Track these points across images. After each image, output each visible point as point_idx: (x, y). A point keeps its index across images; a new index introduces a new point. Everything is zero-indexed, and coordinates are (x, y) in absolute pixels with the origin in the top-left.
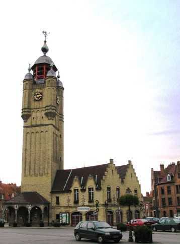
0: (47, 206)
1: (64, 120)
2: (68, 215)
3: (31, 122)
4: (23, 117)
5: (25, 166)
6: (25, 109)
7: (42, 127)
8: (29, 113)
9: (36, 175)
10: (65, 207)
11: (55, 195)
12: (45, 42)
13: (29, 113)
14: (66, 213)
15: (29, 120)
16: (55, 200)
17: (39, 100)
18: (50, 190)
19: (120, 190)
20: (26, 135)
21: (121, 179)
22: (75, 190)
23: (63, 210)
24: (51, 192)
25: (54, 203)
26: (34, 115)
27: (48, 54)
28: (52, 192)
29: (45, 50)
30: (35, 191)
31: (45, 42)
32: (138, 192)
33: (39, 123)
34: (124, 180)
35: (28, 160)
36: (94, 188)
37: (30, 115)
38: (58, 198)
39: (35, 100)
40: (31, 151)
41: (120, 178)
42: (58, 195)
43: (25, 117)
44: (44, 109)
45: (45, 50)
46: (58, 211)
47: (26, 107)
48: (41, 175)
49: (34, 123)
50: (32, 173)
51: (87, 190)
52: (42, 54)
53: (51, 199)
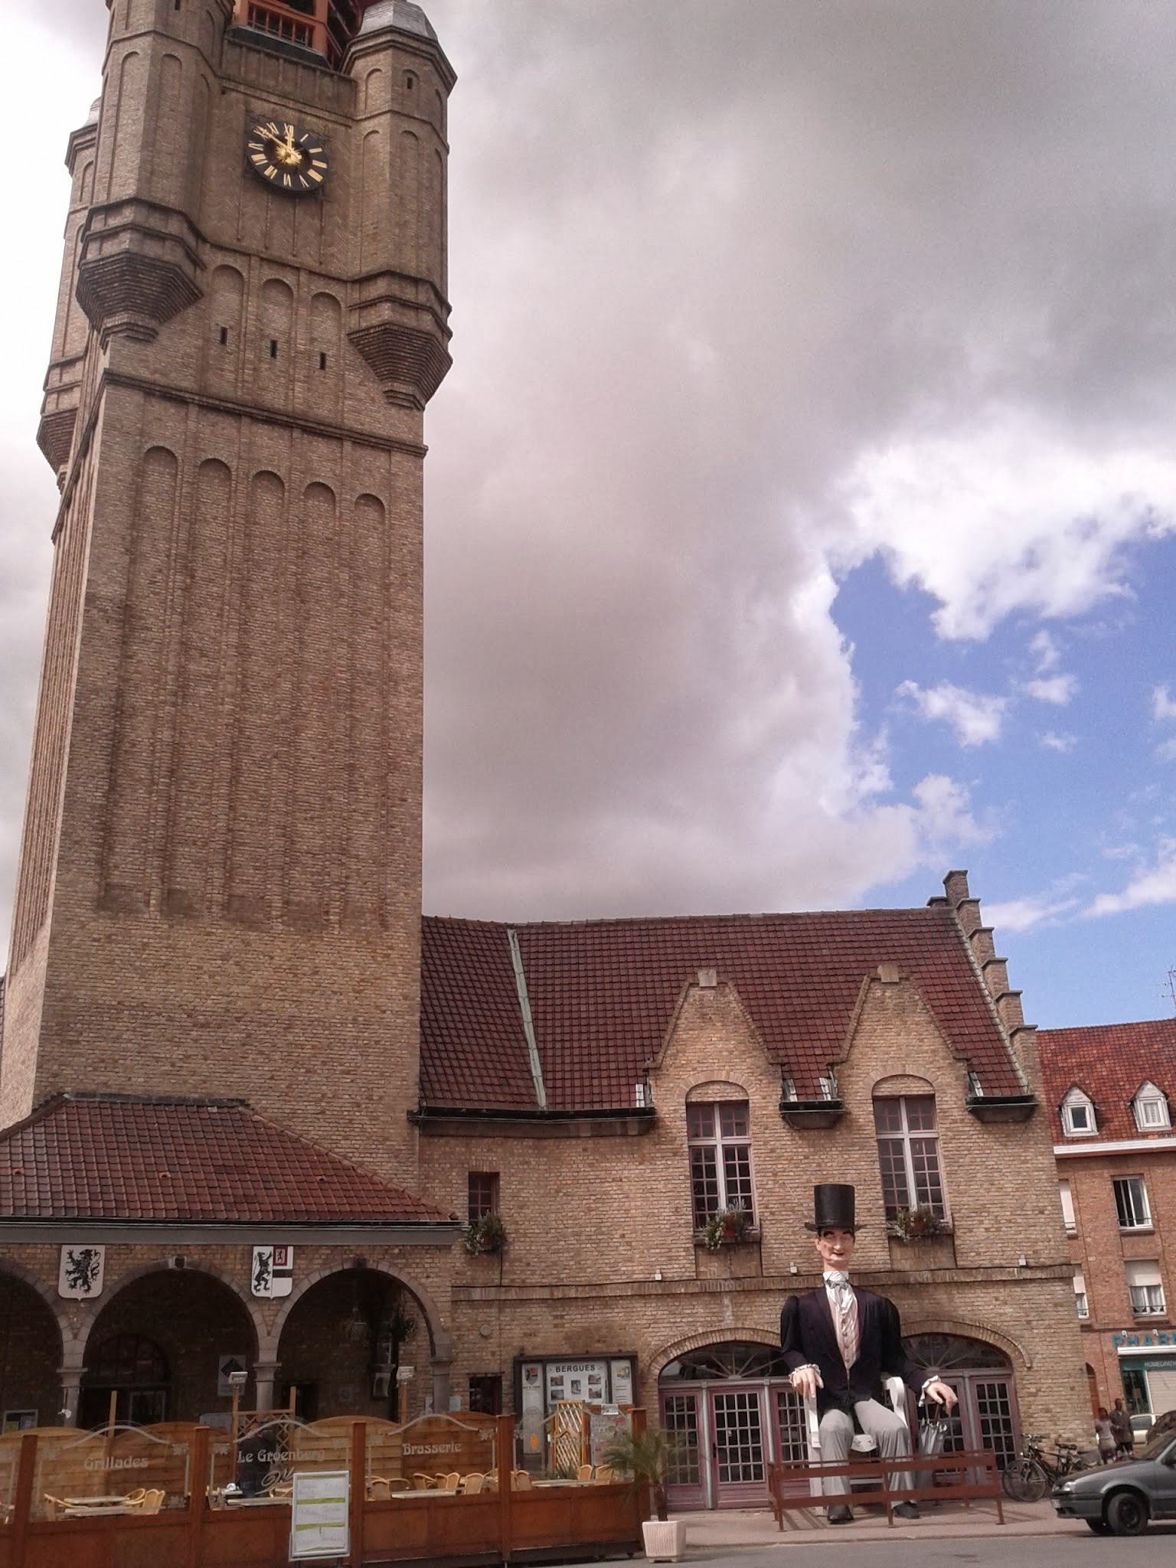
6: (154, 207)
7: (322, 448)
11: (458, 1147)
20: (140, 473)
22: (698, 1113)
24: (413, 1119)
33: (297, 398)
36: (951, 1101)
38: (483, 1186)
39: (254, 175)
42: (486, 1155)
49: (224, 383)
51: (862, 1112)
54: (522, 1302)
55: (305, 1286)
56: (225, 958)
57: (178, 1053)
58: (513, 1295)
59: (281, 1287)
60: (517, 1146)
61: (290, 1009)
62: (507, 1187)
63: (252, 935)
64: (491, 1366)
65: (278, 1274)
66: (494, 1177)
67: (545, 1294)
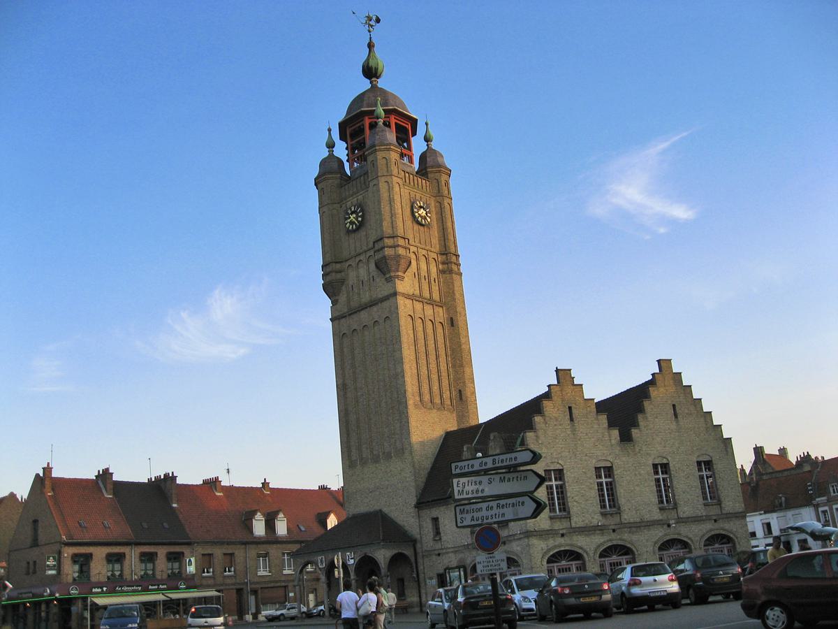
0: (408, 552)
1: (462, 269)
2: (462, 569)
3: (349, 301)
4: (326, 288)
5: (348, 435)
7: (375, 309)
8: (339, 276)
9: (376, 460)
10: (456, 551)
12: (371, 46)
13: (339, 276)
14: (458, 567)
15: (343, 298)
16: (428, 526)
17: (358, 228)
18: (413, 501)
19: (617, 472)
21: (615, 433)
23: (453, 560)
25: (427, 540)
26: (352, 276)
27: (381, 83)
28: (421, 505)
29: (370, 72)
30: (377, 508)
31: (371, 46)
32: (718, 466)
33: (366, 298)
34: (634, 432)
35: (353, 417)
37: (342, 282)
40: (356, 389)
41: (611, 425)
42: (435, 512)
43: (331, 288)
44: (372, 253)
45: (370, 72)
46: (439, 565)
47: (328, 259)
48: (388, 456)
49: (354, 304)
50: (366, 453)
52: (365, 84)
53: (420, 527)
54: (447, 553)
55: (357, 561)
56: (373, 473)
57: (368, 500)
58: (444, 551)
59: (352, 562)
60: (442, 509)
61: (387, 483)
62: (441, 520)
63: (377, 465)
64: (441, 571)
65: (352, 559)
66: (438, 518)
67: (452, 550)
